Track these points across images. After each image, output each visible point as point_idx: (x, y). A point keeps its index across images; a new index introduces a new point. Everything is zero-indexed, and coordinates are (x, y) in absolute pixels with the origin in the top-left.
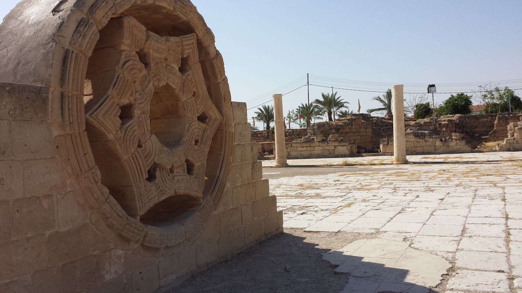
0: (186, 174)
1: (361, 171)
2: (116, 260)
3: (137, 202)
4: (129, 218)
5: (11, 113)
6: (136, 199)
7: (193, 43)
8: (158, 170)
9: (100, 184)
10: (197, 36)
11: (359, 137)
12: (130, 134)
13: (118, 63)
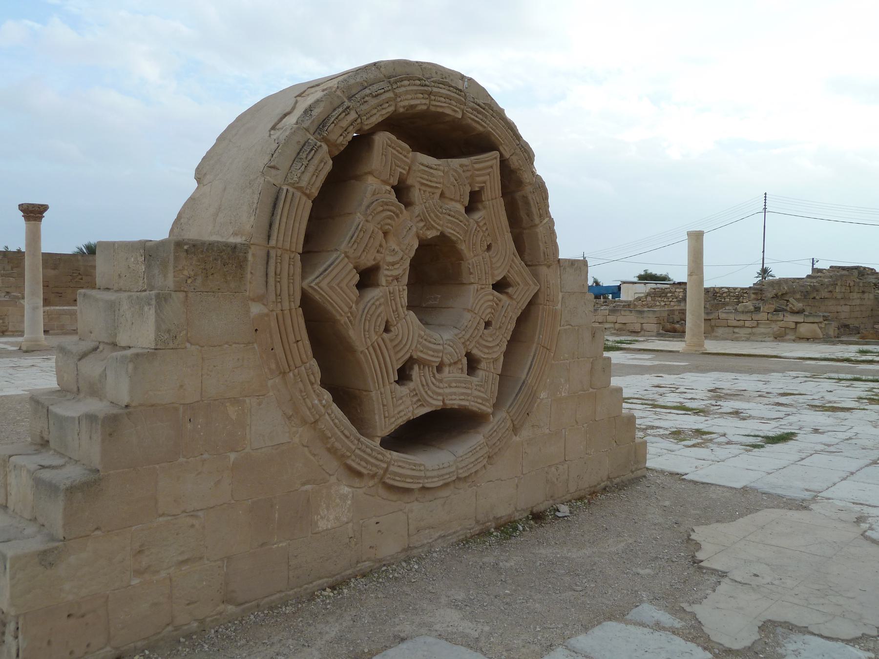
1: (834, 372)
2: (338, 500)
3: (377, 417)
4: (363, 439)
5: (189, 281)
6: (376, 412)
7: (492, 167)
8: (416, 367)
9: (317, 387)
10: (501, 155)
11: (846, 309)
12: (371, 312)
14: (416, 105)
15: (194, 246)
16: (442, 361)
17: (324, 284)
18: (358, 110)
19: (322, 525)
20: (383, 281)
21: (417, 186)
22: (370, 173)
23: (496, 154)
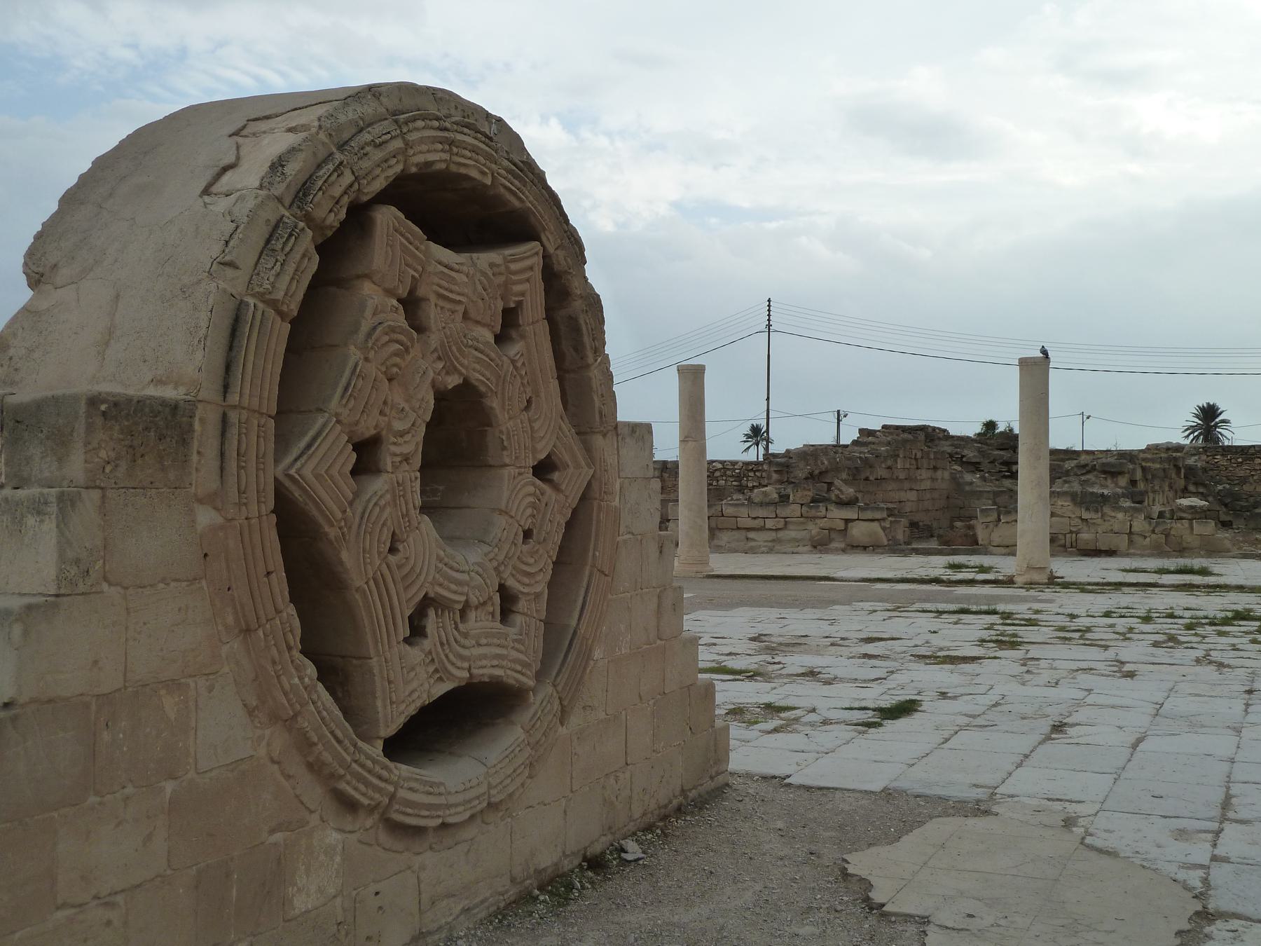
0: (498, 624)
1: (925, 601)
2: (322, 857)
3: (379, 703)
4: (360, 743)
5: (108, 470)
6: (379, 694)
7: (531, 268)
8: (431, 613)
9: (296, 654)
11: (912, 496)
12: (373, 519)
13: (356, 331)
14: (432, 163)
15: (116, 404)
16: (467, 601)
17: (307, 472)
18: (355, 169)
19: (301, 904)
20: (387, 462)
21: (433, 299)
22: (367, 276)
23: (534, 246)
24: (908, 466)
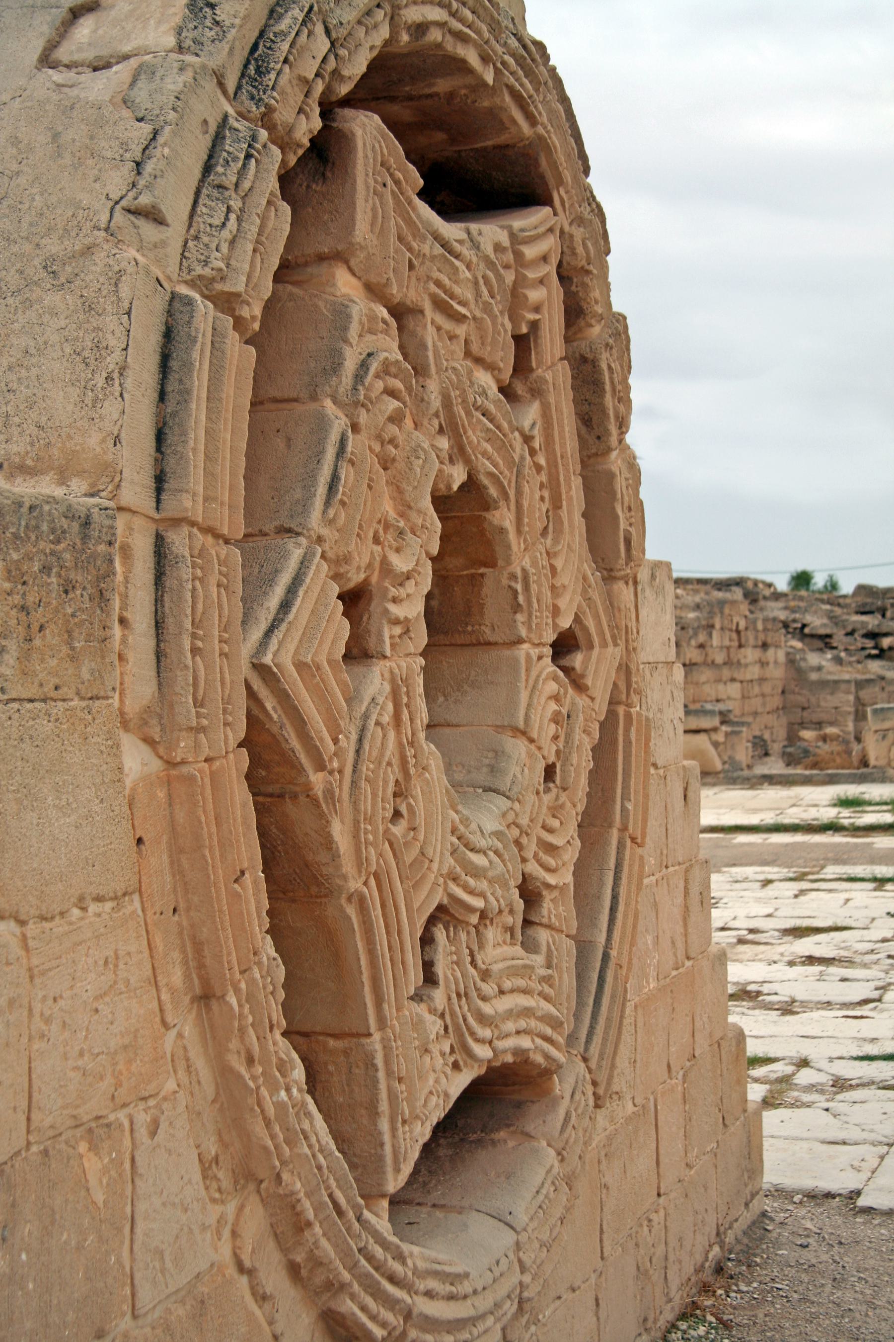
0: (518, 950)
11: (734, 690)
13: (336, 368)
17: (287, 660)
21: (429, 311)
22: (339, 257)
24: (727, 643)
